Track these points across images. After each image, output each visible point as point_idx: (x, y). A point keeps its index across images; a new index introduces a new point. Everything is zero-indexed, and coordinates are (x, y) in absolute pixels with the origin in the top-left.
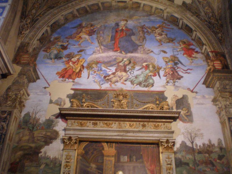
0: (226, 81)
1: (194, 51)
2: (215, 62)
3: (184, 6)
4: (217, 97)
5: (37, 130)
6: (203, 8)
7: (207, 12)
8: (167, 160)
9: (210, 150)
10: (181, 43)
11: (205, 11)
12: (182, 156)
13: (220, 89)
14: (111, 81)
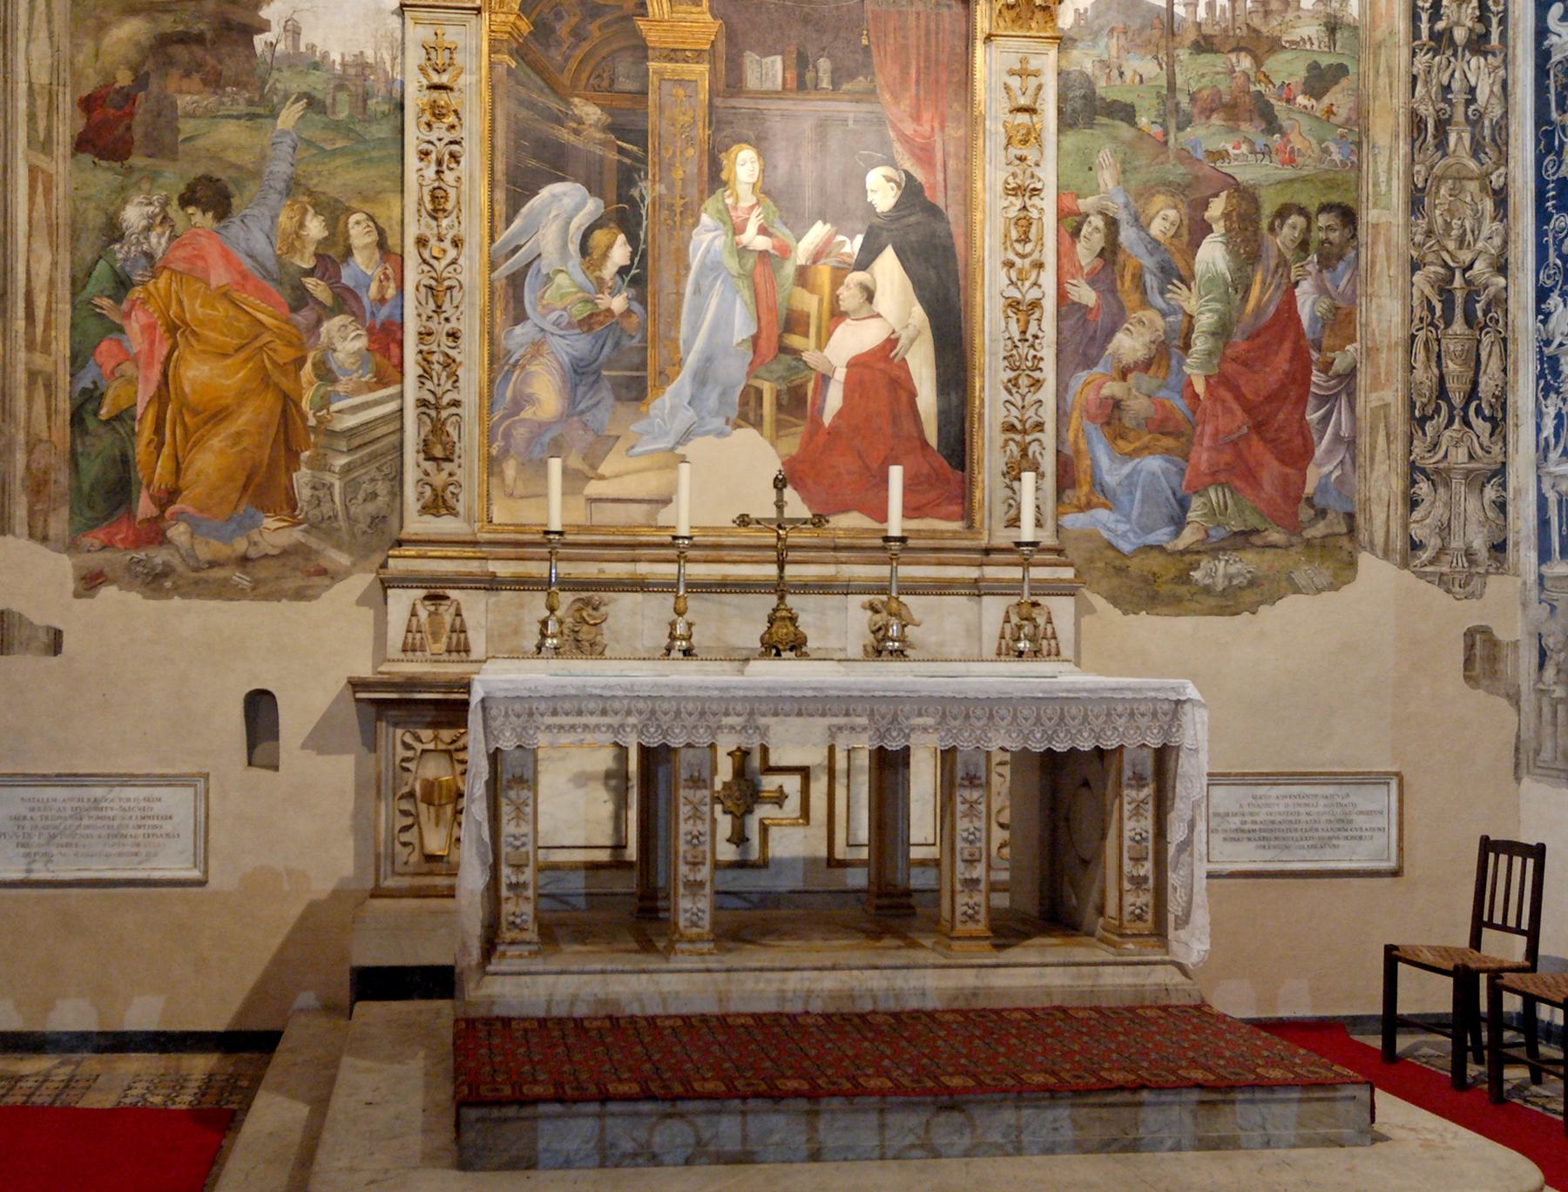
8: (1015, 82)
9: (1264, 30)
12: (1101, 61)
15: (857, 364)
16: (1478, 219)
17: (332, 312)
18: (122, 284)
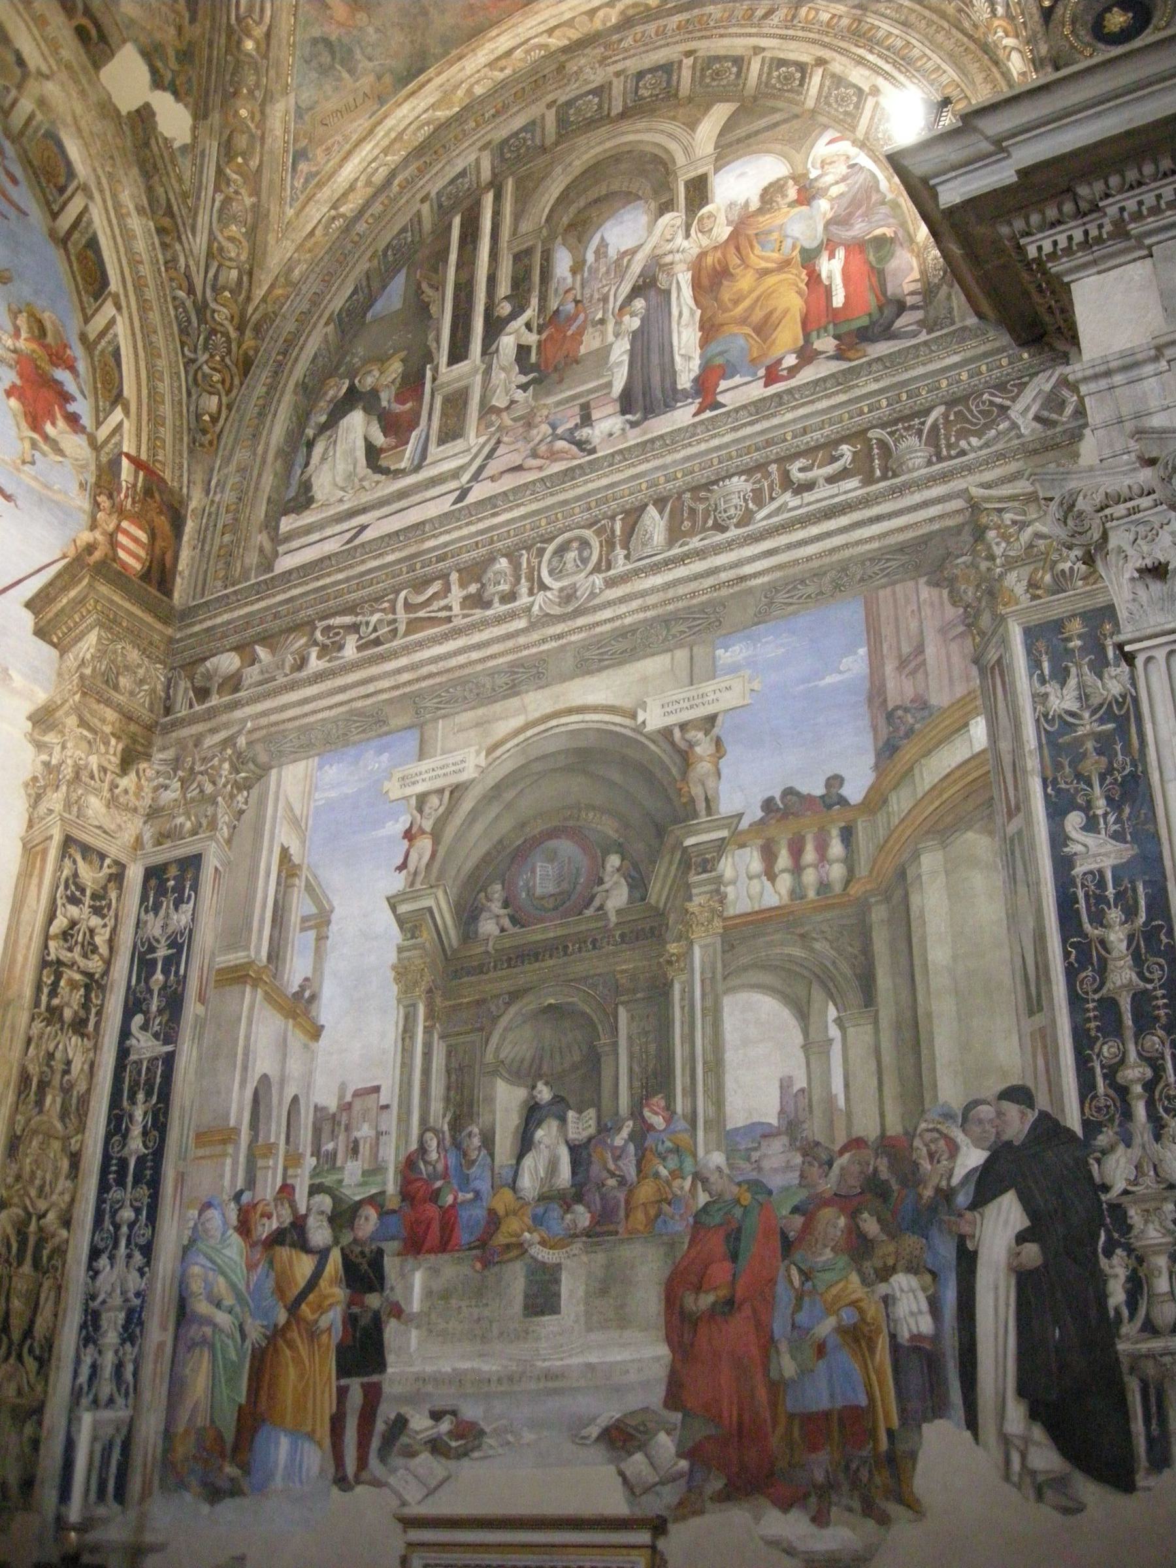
0: (129, 647)
1: (62, 408)
2: (125, 524)
3: (133, 129)
4: (62, 704)
6: (219, 220)
7: (221, 249)
10: (22, 321)
11: (220, 238)
13: (88, 671)
16: (56, 1176)
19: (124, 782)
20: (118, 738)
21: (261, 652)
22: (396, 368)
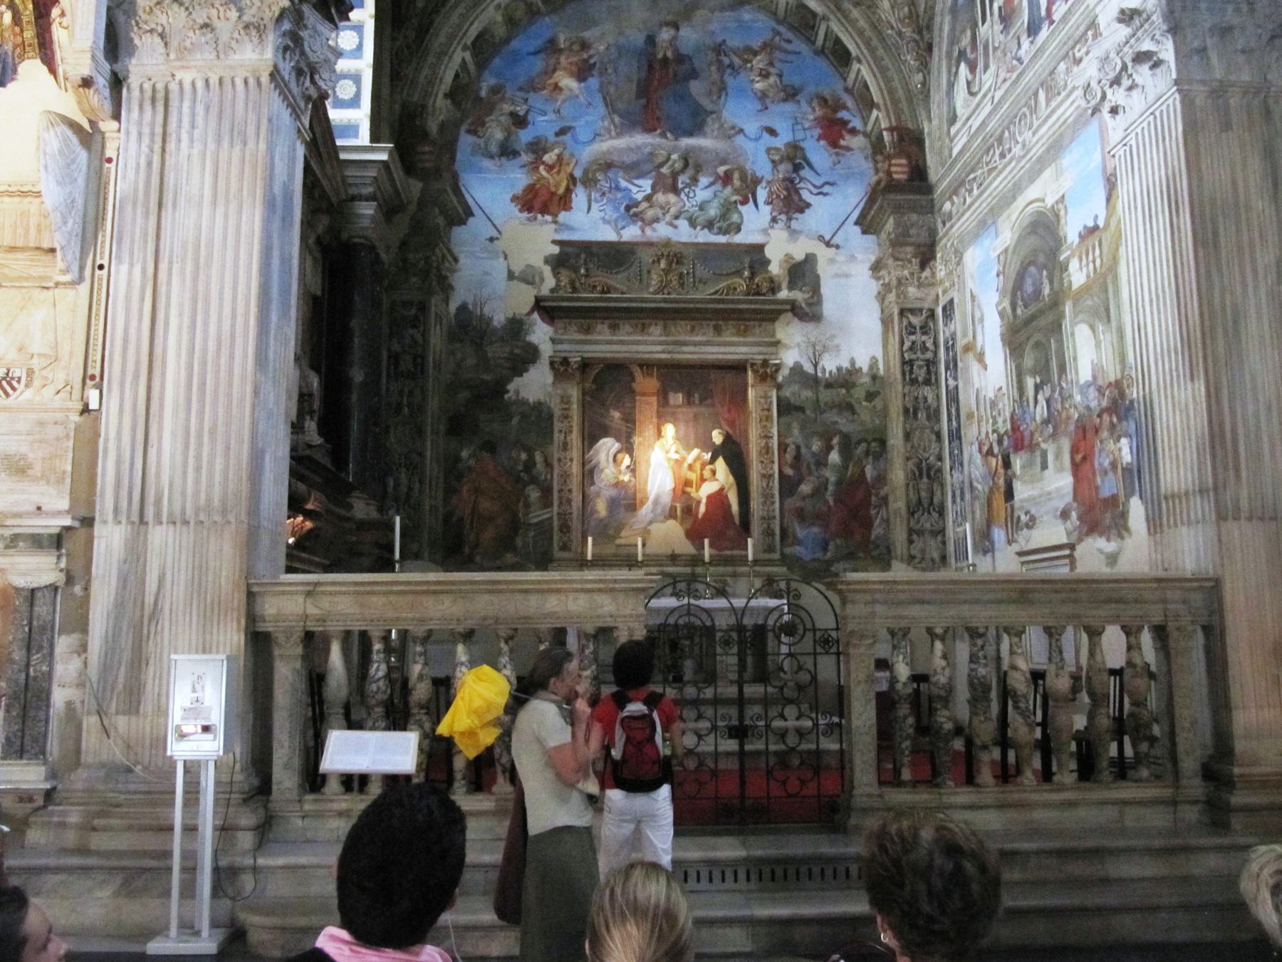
2: (893, 162)
5: (491, 343)
8: (762, 401)
10: (815, 104)
13: (893, 236)
14: (643, 220)
15: (709, 497)
16: (930, 441)
17: (529, 484)
18: (460, 477)
19: (924, 274)
20: (915, 257)
21: (954, 198)
22: (969, 33)
